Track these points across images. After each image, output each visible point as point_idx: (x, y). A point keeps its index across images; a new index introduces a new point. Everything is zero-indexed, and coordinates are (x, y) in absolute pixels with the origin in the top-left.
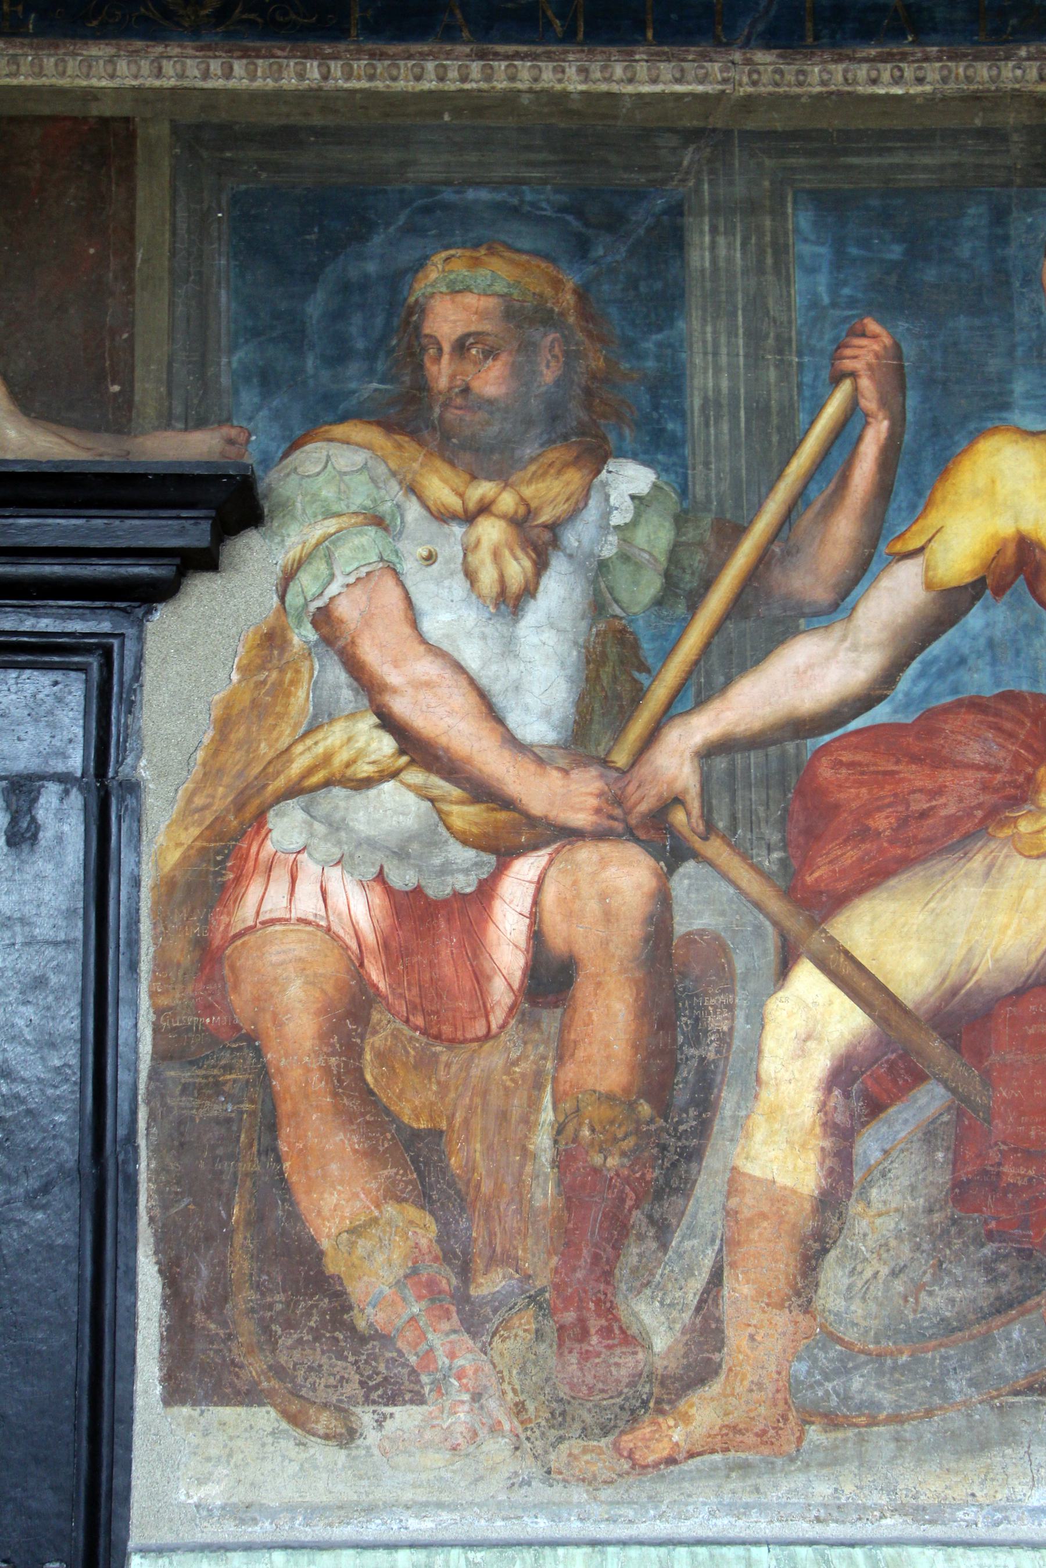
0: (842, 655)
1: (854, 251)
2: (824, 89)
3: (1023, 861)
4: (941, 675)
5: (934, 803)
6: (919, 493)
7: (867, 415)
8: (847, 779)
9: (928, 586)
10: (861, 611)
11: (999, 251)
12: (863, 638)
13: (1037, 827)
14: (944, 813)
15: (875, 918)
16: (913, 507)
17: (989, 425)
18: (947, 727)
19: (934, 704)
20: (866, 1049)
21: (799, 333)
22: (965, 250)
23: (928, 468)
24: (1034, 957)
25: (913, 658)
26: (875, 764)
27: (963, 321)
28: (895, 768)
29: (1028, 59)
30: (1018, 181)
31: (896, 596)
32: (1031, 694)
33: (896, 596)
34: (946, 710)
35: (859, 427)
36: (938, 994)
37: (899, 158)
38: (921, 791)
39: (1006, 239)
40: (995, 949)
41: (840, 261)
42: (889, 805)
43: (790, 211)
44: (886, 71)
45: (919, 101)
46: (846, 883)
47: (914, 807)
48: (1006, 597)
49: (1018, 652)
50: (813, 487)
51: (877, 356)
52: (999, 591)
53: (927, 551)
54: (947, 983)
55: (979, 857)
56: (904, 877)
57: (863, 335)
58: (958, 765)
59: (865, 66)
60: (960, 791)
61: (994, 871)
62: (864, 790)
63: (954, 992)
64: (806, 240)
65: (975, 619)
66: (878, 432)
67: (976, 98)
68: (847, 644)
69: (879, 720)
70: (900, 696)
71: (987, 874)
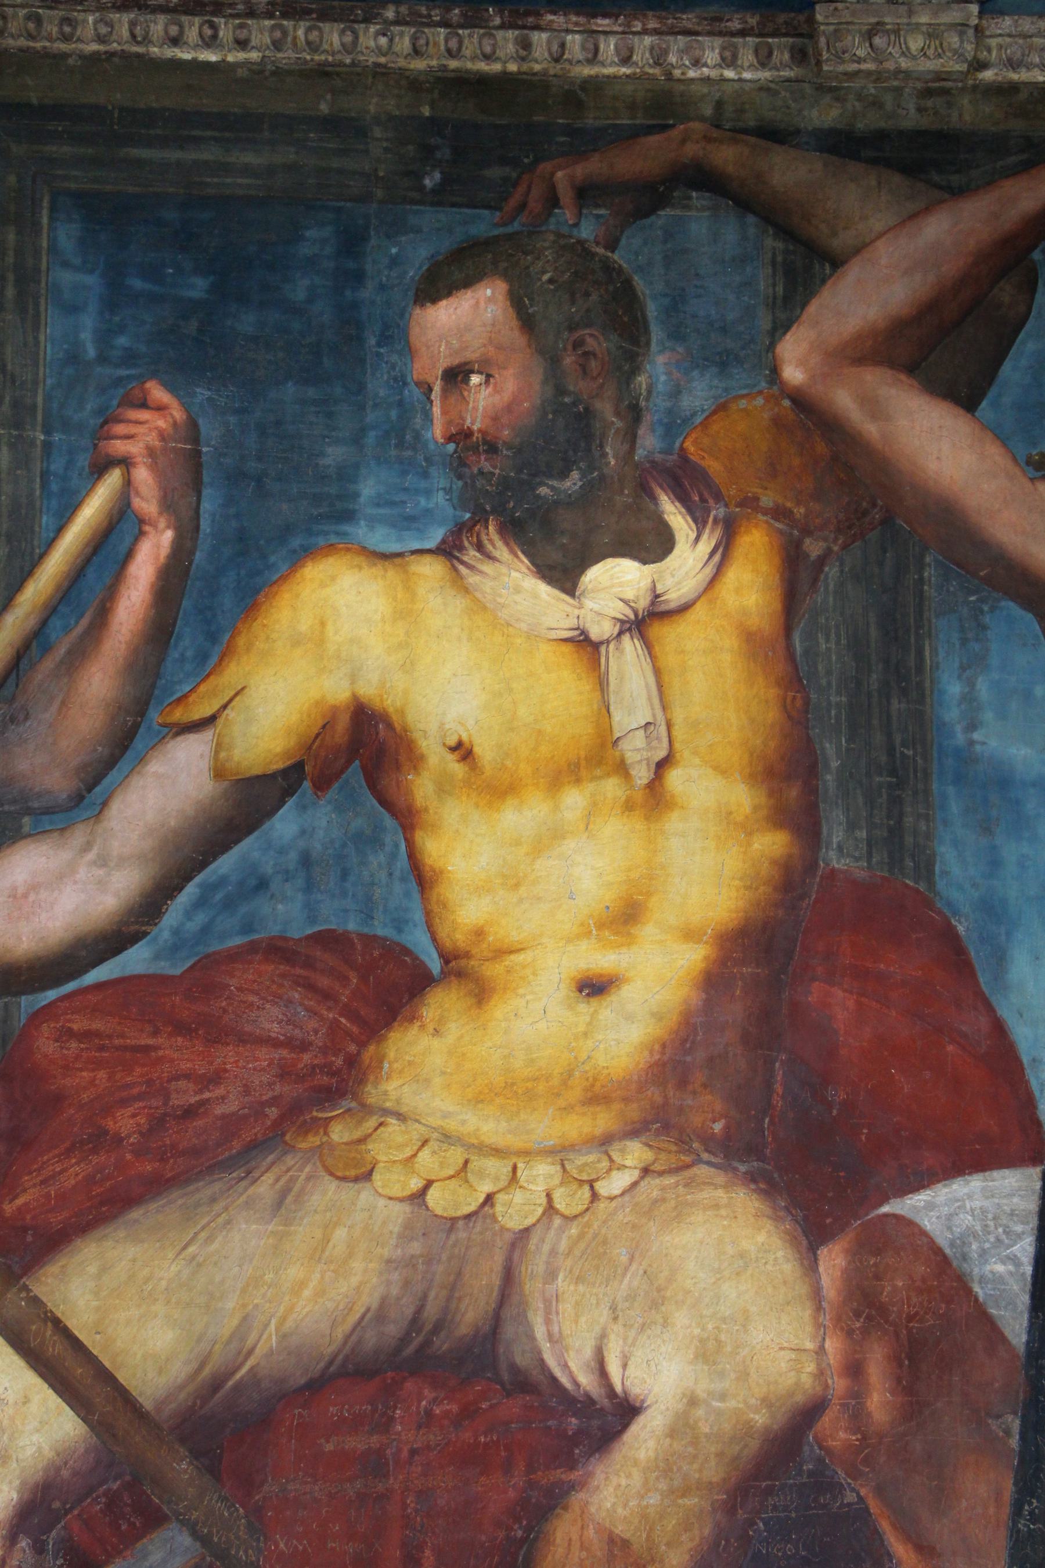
0: (82, 873)
1: (137, 284)
2: (102, 48)
3: (332, 1185)
4: (229, 905)
5: (207, 1095)
6: (213, 638)
7: (142, 521)
8: (77, 1058)
9: (219, 773)
10: (115, 807)
11: (348, 293)
12: (116, 847)
13: (358, 1134)
14: (219, 1110)
15: (104, 1270)
16: (202, 657)
17: (321, 541)
18: (233, 982)
19: (216, 946)
20: (75, 1473)
21: (48, 398)
22: (299, 290)
23: (227, 600)
24: (340, 1333)
25: (188, 879)
26: (122, 1036)
27: (290, 389)
28: (151, 1042)
29: (397, 22)
30: (380, 193)
31: (169, 785)
32: (362, 936)
33: (169, 785)
34: (233, 956)
35: (128, 540)
36: (191, 1388)
37: (208, 154)
38: (187, 1076)
39: (358, 277)
40: (284, 1319)
41: (115, 297)
42: (139, 1097)
43: (45, 220)
44: (193, 28)
45: (241, 73)
46: (65, 1214)
47: (176, 1101)
48: (332, 793)
49: (344, 875)
50: (56, 622)
51: (162, 436)
52: (322, 785)
53: (220, 722)
54: (207, 1371)
55: (269, 1178)
56: (153, 1206)
57: (144, 405)
58: (244, 1039)
59: (162, 19)
60: (247, 1077)
61: (290, 1199)
62: (102, 1074)
63: (216, 1384)
64: (66, 265)
65: (285, 824)
66: (158, 546)
67: (323, 73)
68: (91, 856)
69: (139, 969)
70: (166, 935)
71: (279, 1203)
